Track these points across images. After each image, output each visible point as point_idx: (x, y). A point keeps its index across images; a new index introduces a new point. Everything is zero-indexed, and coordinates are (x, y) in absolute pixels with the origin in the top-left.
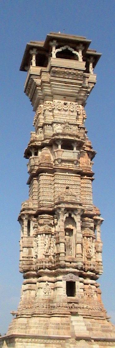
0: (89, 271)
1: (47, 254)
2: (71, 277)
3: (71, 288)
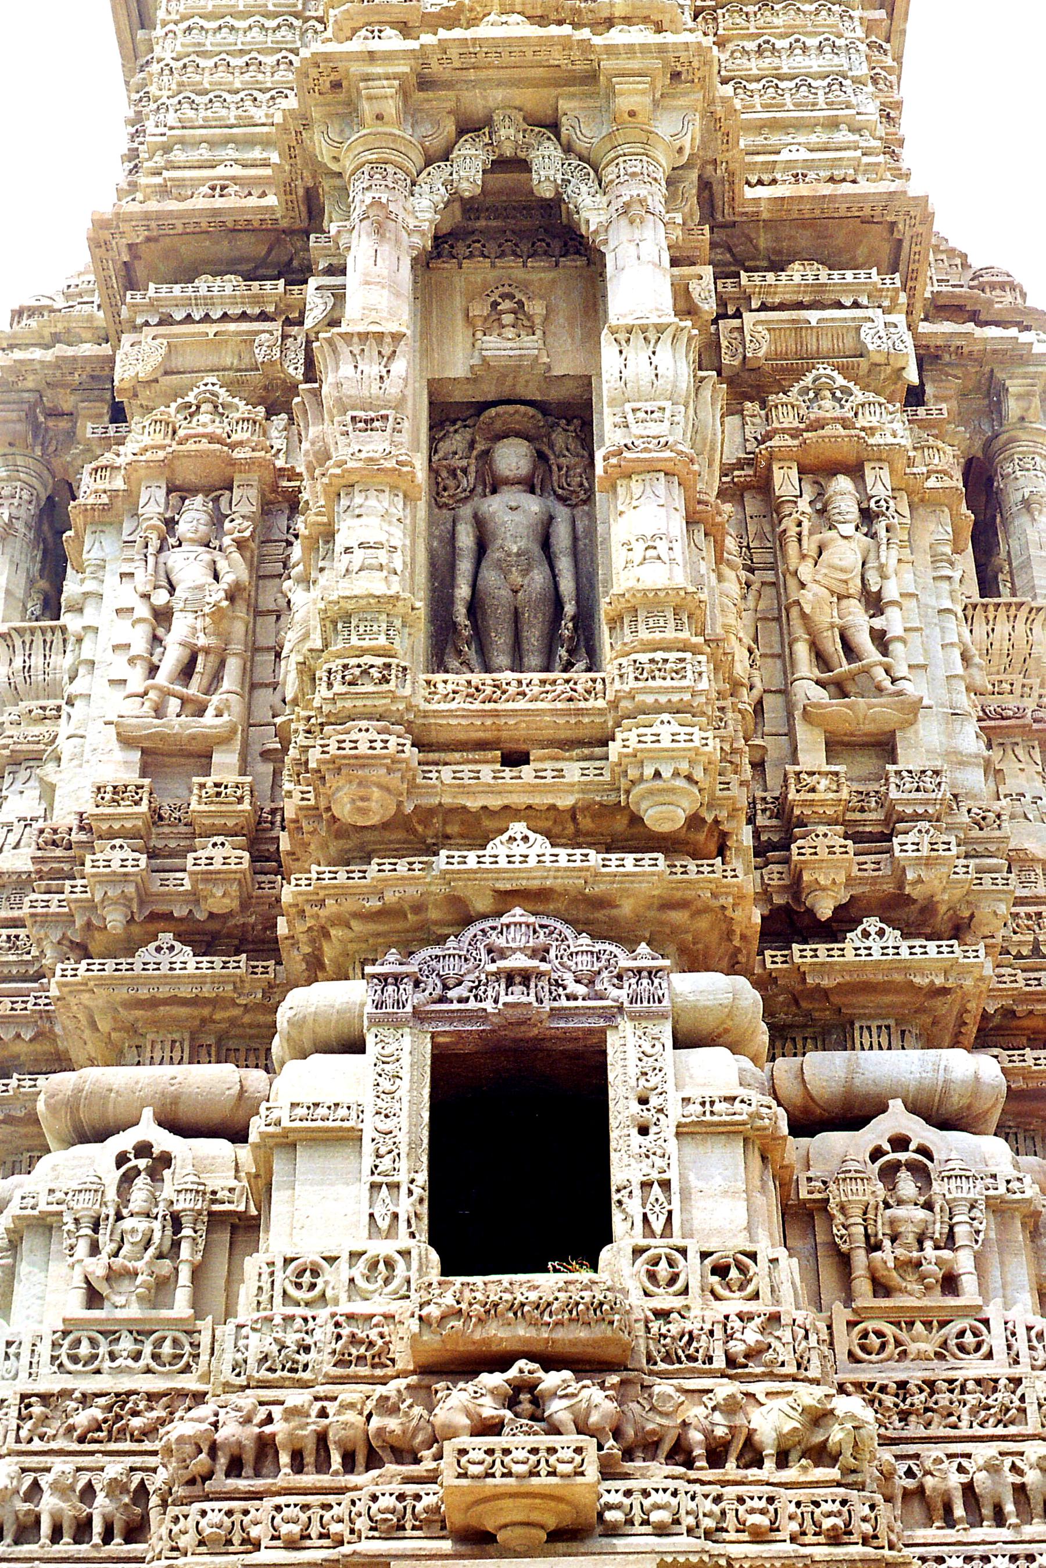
0: (872, 924)
1: (177, 723)
2: (519, 961)
3: (517, 1155)
